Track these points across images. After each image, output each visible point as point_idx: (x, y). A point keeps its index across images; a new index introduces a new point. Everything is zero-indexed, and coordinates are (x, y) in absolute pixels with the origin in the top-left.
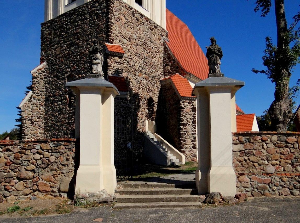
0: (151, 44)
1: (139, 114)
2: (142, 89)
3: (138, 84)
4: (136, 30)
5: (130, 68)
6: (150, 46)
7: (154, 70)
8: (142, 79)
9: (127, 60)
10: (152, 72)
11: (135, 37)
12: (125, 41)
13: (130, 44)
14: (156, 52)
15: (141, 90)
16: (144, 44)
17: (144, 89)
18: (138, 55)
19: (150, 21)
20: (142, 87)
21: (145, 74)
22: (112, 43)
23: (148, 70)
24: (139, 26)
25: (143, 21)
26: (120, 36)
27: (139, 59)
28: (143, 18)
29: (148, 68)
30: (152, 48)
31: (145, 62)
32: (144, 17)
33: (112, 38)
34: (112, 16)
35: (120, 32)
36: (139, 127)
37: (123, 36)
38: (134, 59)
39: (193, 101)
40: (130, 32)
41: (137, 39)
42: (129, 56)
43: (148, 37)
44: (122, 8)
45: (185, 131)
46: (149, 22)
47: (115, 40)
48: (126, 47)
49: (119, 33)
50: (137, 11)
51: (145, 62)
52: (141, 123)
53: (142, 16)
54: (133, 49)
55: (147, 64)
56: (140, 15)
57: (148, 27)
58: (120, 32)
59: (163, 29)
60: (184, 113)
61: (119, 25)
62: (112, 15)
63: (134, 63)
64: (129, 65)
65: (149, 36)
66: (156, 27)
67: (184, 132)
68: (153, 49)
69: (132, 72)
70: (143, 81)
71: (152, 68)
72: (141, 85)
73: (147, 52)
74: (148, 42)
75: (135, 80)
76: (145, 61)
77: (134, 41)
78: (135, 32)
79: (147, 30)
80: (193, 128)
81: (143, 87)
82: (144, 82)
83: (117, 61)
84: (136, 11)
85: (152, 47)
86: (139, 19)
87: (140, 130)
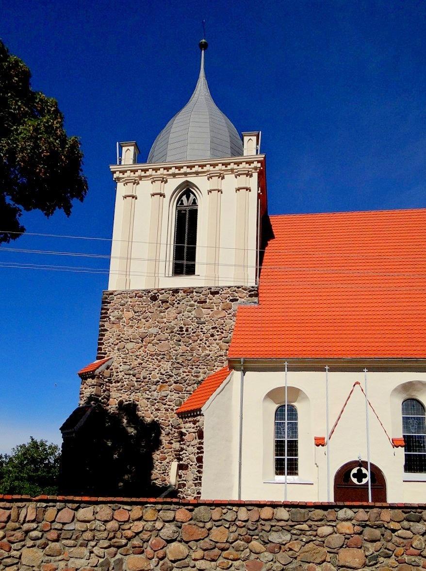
0: (198, 327)
1: (156, 456)
2: (167, 410)
3: (157, 404)
4: (157, 320)
5: (136, 384)
6: (194, 333)
7: (201, 371)
8: (164, 394)
9: (131, 372)
10: (196, 374)
11: (153, 330)
12: (130, 346)
13: (142, 347)
14: (212, 335)
15: (164, 412)
16: (179, 334)
17: (172, 410)
18: (159, 358)
19: (197, 290)
20: (165, 406)
21: (175, 383)
22: (104, 357)
23: (185, 374)
24: (167, 311)
25: (178, 298)
26: (120, 342)
27: (160, 364)
28: (181, 294)
29: (186, 371)
30: (202, 333)
31: (178, 363)
32: (180, 291)
33: (103, 352)
34: (105, 321)
35: (121, 336)
36: (153, 477)
37: (128, 340)
38: (151, 366)
39: (199, 417)
40: (143, 329)
41: (160, 332)
42: (138, 365)
43: (189, 319)
44: (130, 300)
45: (184, 479)
46: (196, 292)
47: (108, 353)
48: (131, 354)
49: (117, 339)
50: (163, 289)
51: (178, 363)
52: (158, 469)
53: (176, 291)
54: (148, 351)
55: (182, 365)
56: (171, 292)
57: (192, 302)
58: (121, 336)
59: (238, 288)
60: (184, 444)
61: (119, 327)
62: (105, 320)
63: (148, 372)
64: (137, 379)
65: (193, 316)
66: (214, 293)
67: (182, 482)
68: (204, 333)
69: (142, 389)
70: (169, 396)
71: (197, 368)
72: (165, 404)
73: (185, 345)
74: (189, 327)
75: (149, 399)
76: (178, 361)
77: (153, 338)
78: (157, 323)
79: (189, 308)
80: (197, 473)
81: (170, 405)
82: (173, 397)
83: (90, 384)
84: (158, 290)
85: (201, 331)
86: (171, 298)
87: (158, 483)
